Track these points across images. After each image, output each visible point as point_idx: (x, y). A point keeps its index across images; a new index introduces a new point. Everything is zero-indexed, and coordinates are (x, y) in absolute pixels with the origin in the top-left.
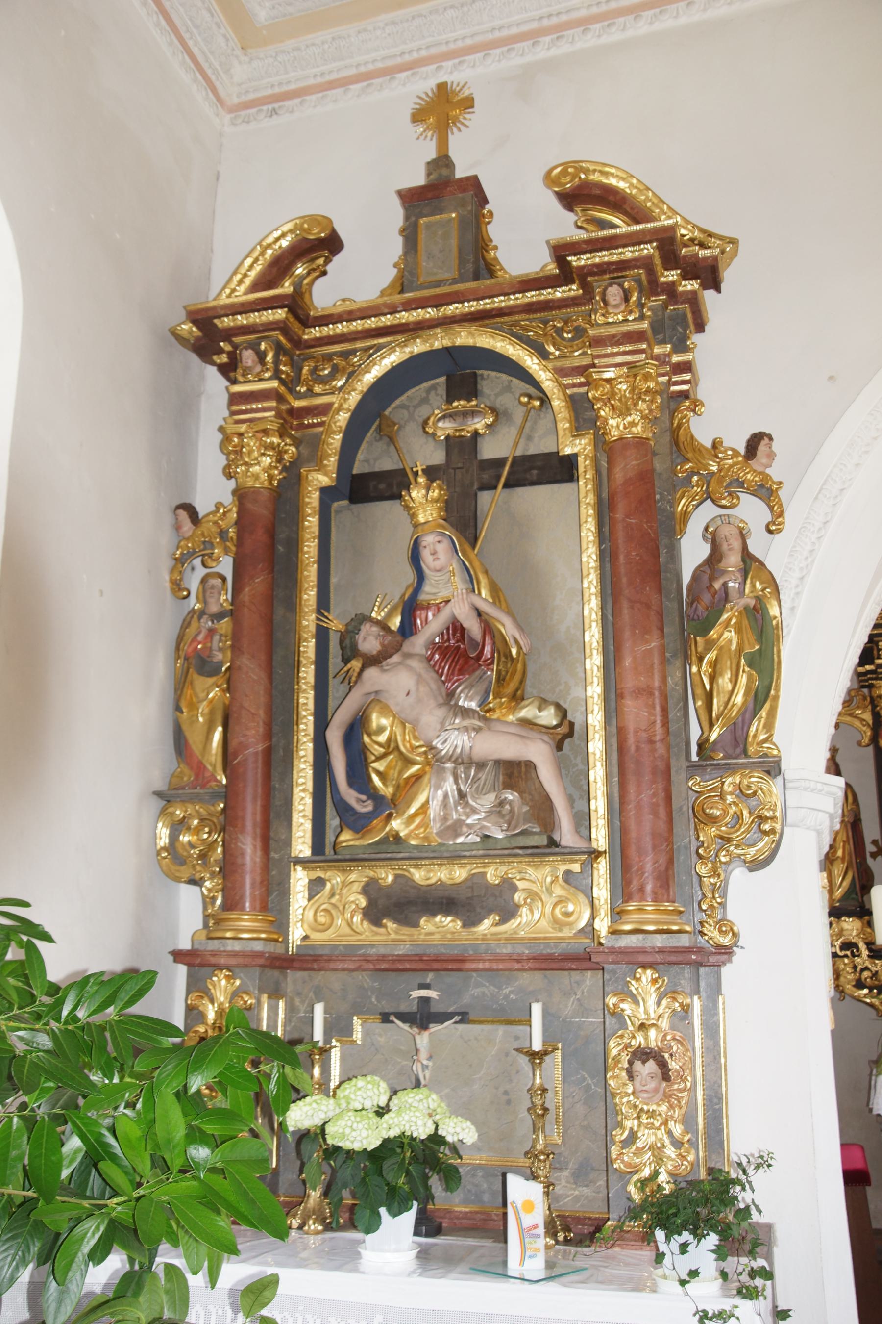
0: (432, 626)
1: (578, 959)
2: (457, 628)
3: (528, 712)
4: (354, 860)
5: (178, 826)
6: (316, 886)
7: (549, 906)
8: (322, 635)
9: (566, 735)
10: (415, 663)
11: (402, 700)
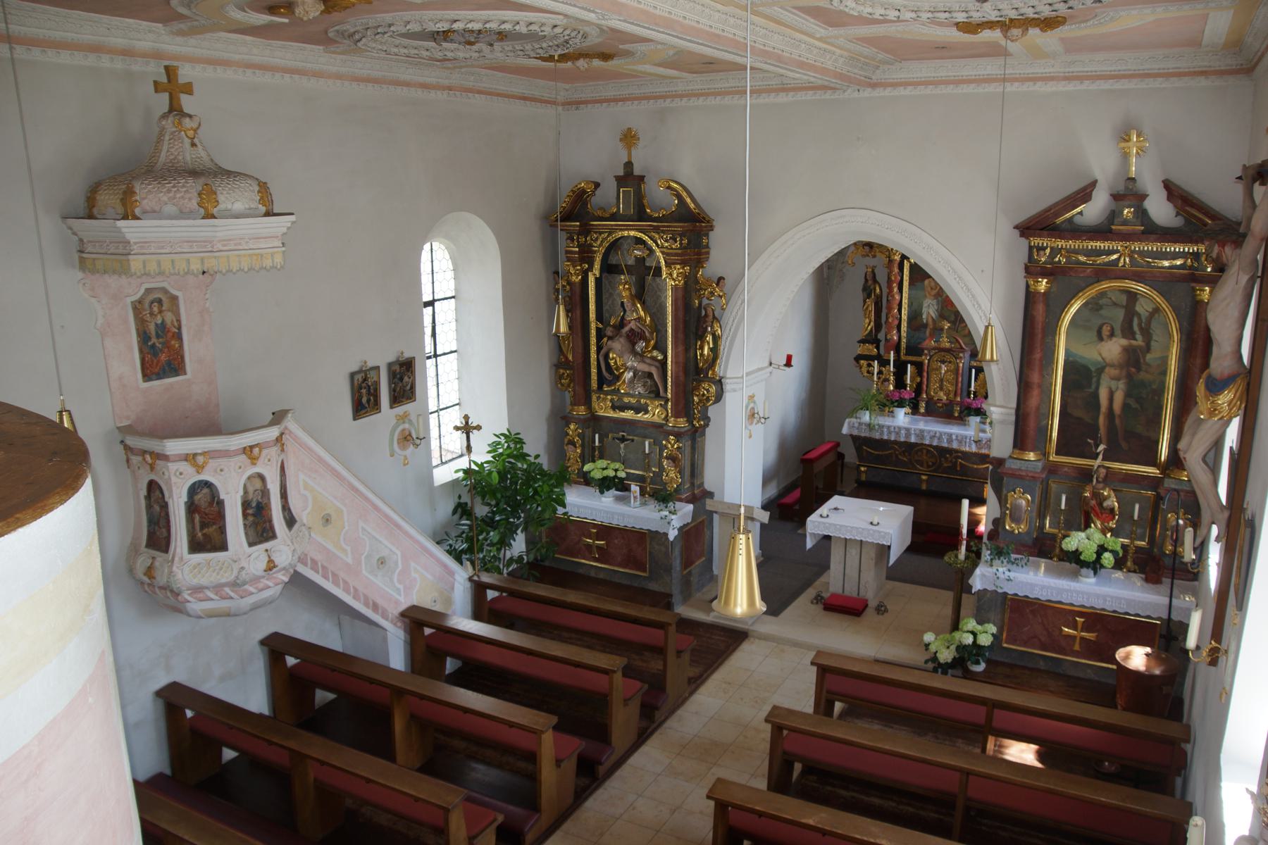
0: (627, 329)
1: (658, 429)
2: (632, 330)
3: (655, 353)
4: (607, 393)
5: (561, 377)
6: (598, 398)
7: (655, 413)
8: (598, 329)
9: (664, 363)
10: (622, 340)
11: (618, 354)
